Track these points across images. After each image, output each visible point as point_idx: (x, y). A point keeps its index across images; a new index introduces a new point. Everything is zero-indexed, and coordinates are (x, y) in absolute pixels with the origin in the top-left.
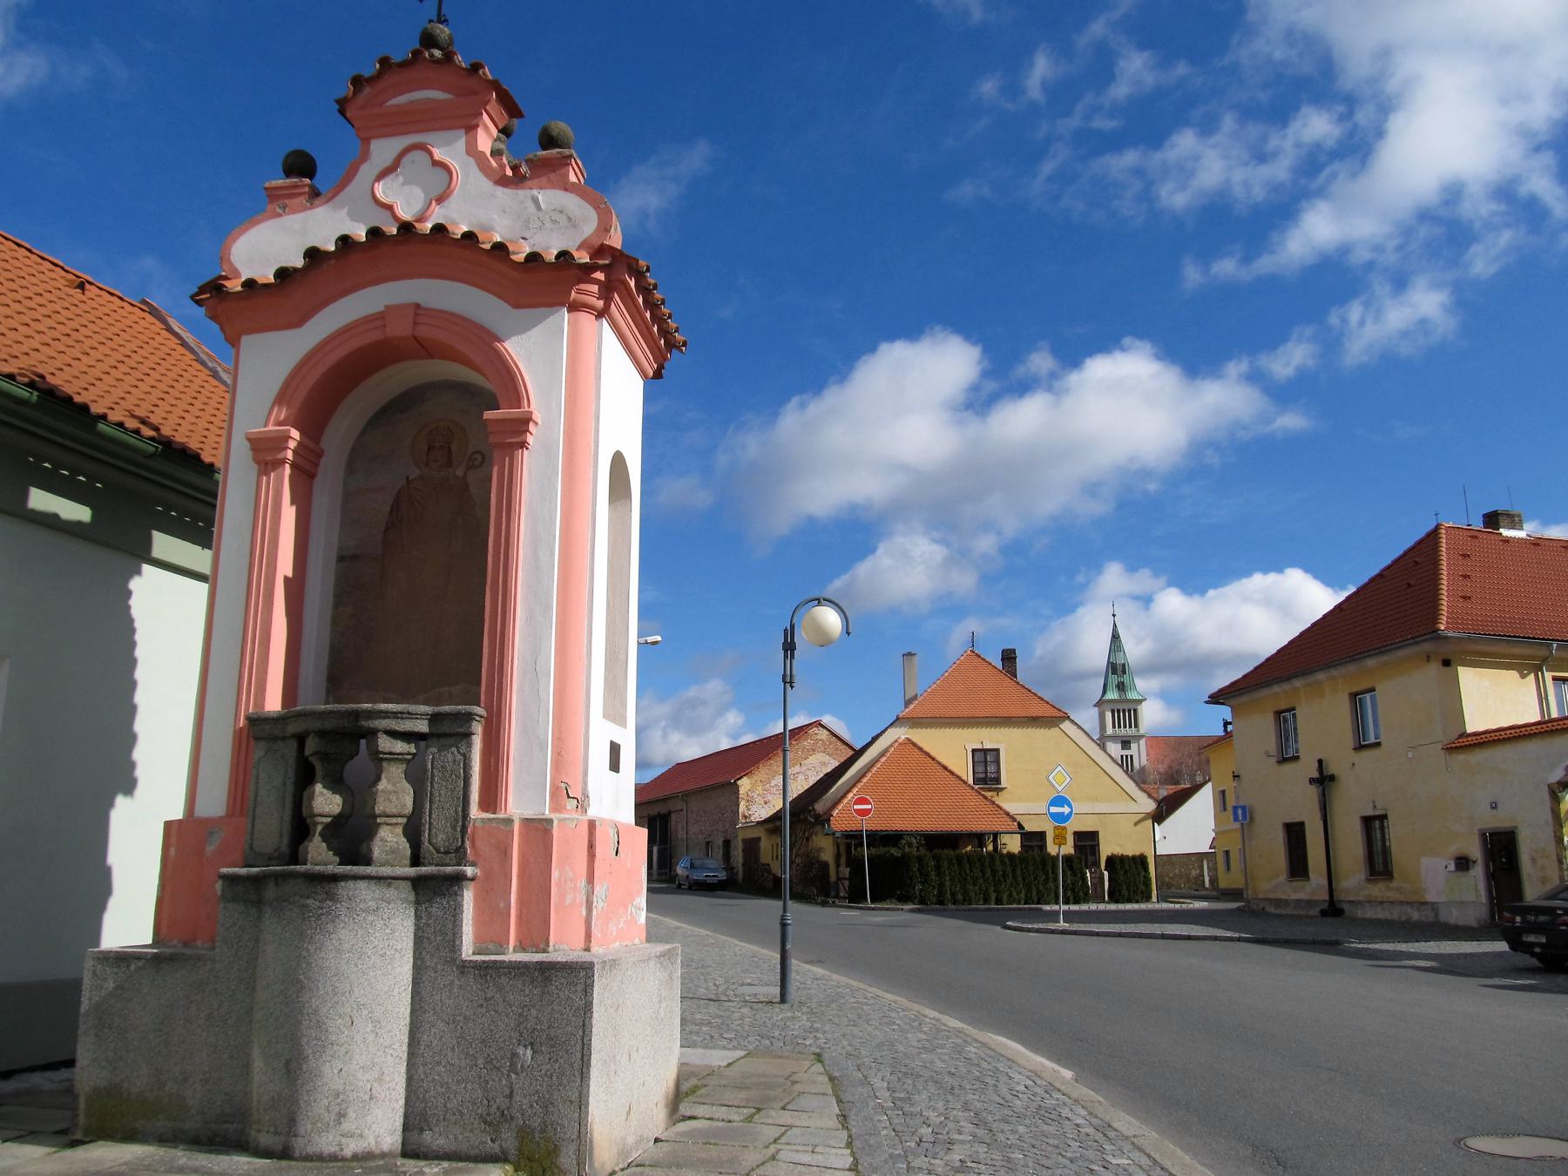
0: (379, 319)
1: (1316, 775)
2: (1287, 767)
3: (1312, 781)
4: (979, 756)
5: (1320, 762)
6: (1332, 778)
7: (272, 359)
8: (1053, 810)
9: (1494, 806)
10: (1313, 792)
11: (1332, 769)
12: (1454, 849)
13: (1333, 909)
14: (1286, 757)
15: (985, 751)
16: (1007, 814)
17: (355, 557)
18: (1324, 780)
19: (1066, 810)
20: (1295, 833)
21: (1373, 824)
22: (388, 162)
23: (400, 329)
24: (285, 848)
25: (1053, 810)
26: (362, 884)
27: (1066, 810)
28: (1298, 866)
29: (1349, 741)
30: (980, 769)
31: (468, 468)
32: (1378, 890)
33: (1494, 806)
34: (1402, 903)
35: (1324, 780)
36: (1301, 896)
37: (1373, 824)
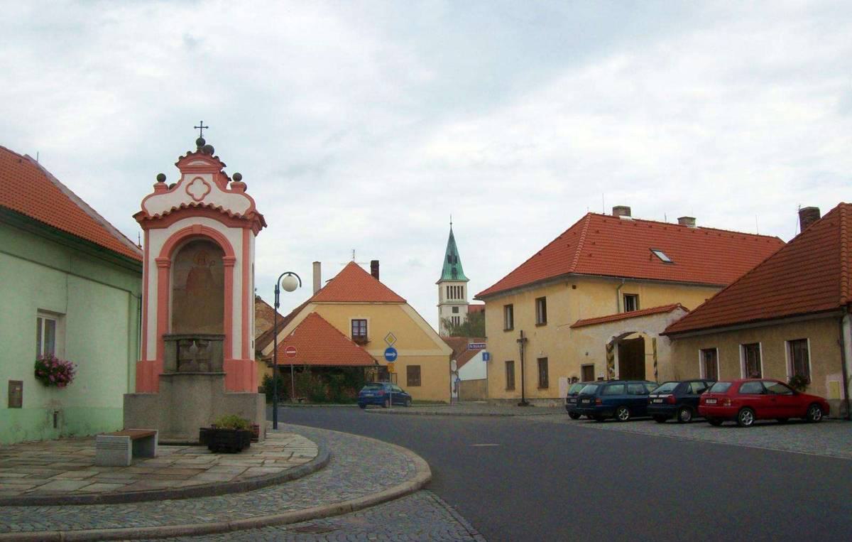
0: (191, 228)
1: (519, 338)
2: (509, 334)
3: (518, 341)
4: (356, 324)
5: (522, 332)
6: (526, 339)
7: (161, 239)
8: (388, 354)
9: (587, 354)
10: (518, 346)
11: (527, 336)
12: (570, 375)
13: (524, 403)
14: (510, 327)
15: (359, 321)
16: (371, 356)
17: (179, 289)
18: (523, 341)
19: (394, 354)
20: (510, 365)
21: (543, 363)
22: (190, 182)
23: (197, 231)
24: (175, 367)
25: (388, 354)
26: (200, 376)
27: (394, 354)
28: (511, 386)
29: (534, 321)
30: (356, 331)
31: (210, 266)
32: (544, 394)
33: (587, 354)
34: (551, 399)
35: (523, 341)
36: (512, 397)
37: (543, 363)
